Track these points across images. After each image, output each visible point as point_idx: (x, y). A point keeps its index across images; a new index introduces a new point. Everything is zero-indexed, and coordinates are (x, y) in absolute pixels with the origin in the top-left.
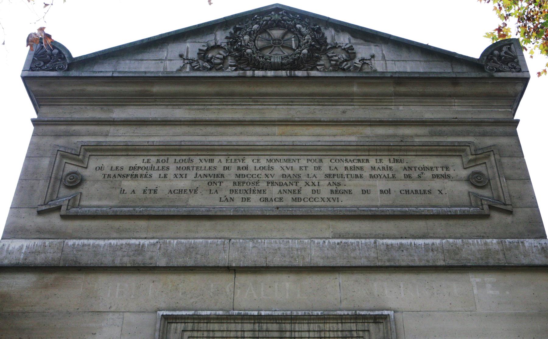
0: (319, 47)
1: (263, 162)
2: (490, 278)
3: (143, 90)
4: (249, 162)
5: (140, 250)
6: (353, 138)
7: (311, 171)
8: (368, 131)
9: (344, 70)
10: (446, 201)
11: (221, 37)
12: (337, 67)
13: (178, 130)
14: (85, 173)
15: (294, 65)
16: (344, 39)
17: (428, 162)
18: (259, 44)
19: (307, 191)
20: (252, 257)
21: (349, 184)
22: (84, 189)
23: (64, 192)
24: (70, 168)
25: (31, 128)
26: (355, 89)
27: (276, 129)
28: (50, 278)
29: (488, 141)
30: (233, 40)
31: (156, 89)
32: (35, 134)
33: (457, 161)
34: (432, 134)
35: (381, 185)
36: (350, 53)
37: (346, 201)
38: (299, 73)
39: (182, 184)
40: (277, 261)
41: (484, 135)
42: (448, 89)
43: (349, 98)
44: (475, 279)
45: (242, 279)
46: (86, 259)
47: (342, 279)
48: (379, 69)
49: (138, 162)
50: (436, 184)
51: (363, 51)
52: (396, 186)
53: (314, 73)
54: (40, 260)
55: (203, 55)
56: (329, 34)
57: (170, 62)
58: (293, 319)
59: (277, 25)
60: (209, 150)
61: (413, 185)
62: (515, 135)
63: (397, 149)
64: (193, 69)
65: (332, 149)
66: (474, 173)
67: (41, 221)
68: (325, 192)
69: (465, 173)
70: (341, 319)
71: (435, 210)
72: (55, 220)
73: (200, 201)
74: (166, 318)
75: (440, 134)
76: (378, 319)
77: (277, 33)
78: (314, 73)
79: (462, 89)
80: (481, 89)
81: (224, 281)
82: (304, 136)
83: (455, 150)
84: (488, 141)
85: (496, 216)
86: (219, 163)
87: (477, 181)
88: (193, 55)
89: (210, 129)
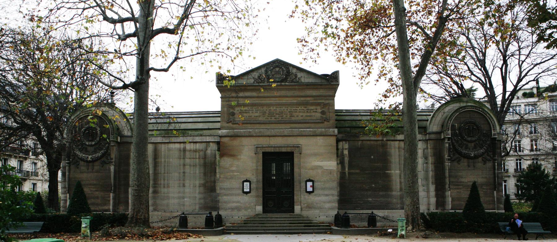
0: (288, 73)
1: (275, 108)
2: (322, 137)
3: (245, 88)
4: (271, 108)
5: (250, 132)
6: (295, 101)
7: (286, 111)
8: (299, 99)
9: (295, 82)
10: (314, 118)
11: (263, 70)
12: (292, 82)
13: (254, 99)
14: (235, 112)
15: (282, 81)
16: (294, 71)
17: (312, 108)
18: (273, 73)
19: (284, 116)
20: (273, 134)
21: (294, 114)
22: (236, 116)
23: (231, 117)
24: (231, 111)
25: (220, 99)
26: (297, 87)
27: (277, 99)
28: (232, 138)
29: (327, 102)
30: (266, 72)
31: (248, 88)
32: (222, 101)
33: (319, 107)
34: (314, 100)
35: (301, 114)
36: (296, 76)
37: (293, 119)
38: (283, 84)
39: (257, 114)
40: (278, 134)
41: (327, 100)
42: (319, 87)
43: (295, 89)
44: (318, 138)
45: (271, 138)
46: (239, 134)
47: (291, 138)
48: (303, 81)
49: (246, 108)
50: (313, 114)
51: (299, 75)
52: (304, 114)
53: (287, 84)
54: (230, 135)
55: (259, 77)
56: (291, 68)
57: (250, 81)
58: (281, 147)
59: (277, 67)
60: (262, 105)
61: (308, 114)
62: (334, 100)
63: (306, 104)
64: (257, 83)
65: (291, 105)
66: (323, 111)
67: (228, 125)
68: (288, 117)
69: (320, 111)
70: (291, 147)
71: (312, 121)
72: (230, 125)
73: (261, 119)
74: (257, 147)
75: (316, 100)
76: (298, 147)
77: (277, 69)
78: (287, 84)
79: (323, 87)
80: (327, 87)
81: (267, 139)
82: (284, 100)
83: (318, 104)
84: (327, 102)
85: (326, 122)
86: (265, 108)
87: (323, 113)
88: (256, 77)
89: (262, 99)
